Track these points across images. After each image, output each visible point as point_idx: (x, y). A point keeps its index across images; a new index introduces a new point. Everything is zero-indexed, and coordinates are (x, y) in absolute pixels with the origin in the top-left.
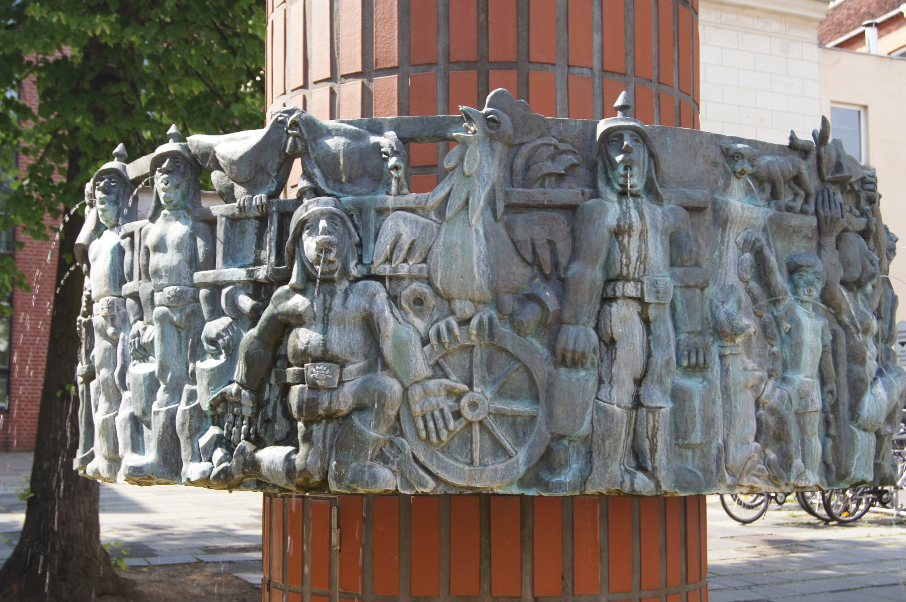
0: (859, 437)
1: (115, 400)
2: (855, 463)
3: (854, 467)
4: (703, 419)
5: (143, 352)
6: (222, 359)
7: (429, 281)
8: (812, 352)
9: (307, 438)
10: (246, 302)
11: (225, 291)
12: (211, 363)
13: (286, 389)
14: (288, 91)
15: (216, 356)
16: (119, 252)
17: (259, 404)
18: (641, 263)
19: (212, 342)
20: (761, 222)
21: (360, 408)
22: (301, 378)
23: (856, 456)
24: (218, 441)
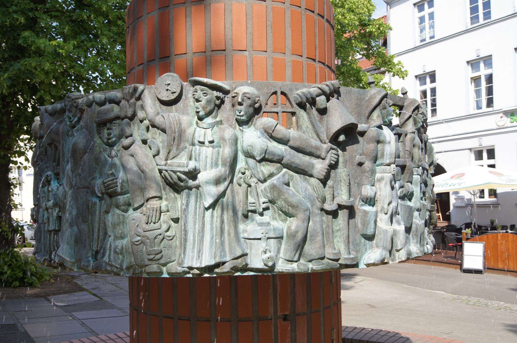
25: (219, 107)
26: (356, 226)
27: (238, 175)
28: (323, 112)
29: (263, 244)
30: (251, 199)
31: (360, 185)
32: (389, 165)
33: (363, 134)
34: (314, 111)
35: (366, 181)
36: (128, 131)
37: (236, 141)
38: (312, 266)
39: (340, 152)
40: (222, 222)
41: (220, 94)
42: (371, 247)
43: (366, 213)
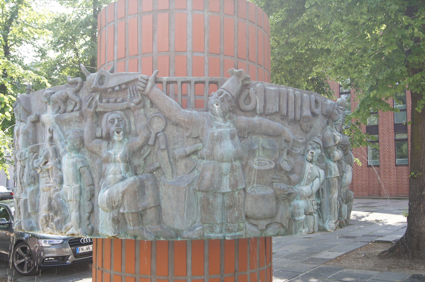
0: (100, 214)
2: (100, 226)
3: (100, 228)
4: (30, 203)
8: (66, 174)
18: (18, 146)
20: (53, 121)
23: (100, 223)
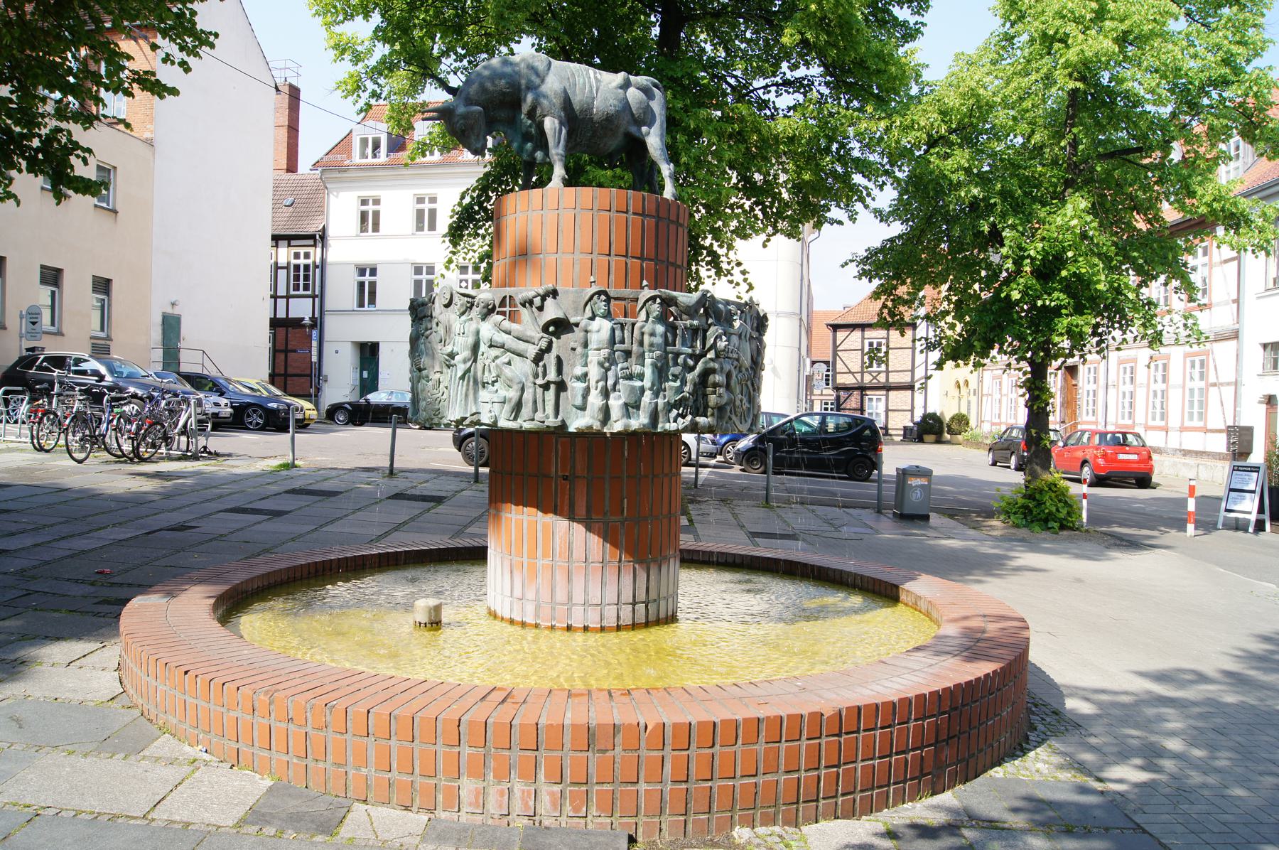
1: (606, 394)
5: (630, 377)
6: (678, 383)
7: (738, 360)
9: (712, 415)
10: (691, 362)
11: (683, 356)
12: (671, 384)
13: (705, 396)
14: (595, 253)
15: (675, 381)
16: (613, 330)
17: (695, 401)
19: (673, 375)
21: (726, 404)
22: (714, 393)
24: (678, 415)
25: (471, 308)
26: (567, 398)
27: (479, 357)
28: (541, 309)
29: (489, 406)
30: (487, 373)
31: (573, 366)
32: (599, 349)
33: (577, 325)
34: (534, 309)
35: (577, 363)
36: (429, 326)
37: (478, 333)
38: (527, 425)
39: (554, 339)
40: (467, 390)
41: (470, 300)
42: (584, 416)
43: (573, 388)
